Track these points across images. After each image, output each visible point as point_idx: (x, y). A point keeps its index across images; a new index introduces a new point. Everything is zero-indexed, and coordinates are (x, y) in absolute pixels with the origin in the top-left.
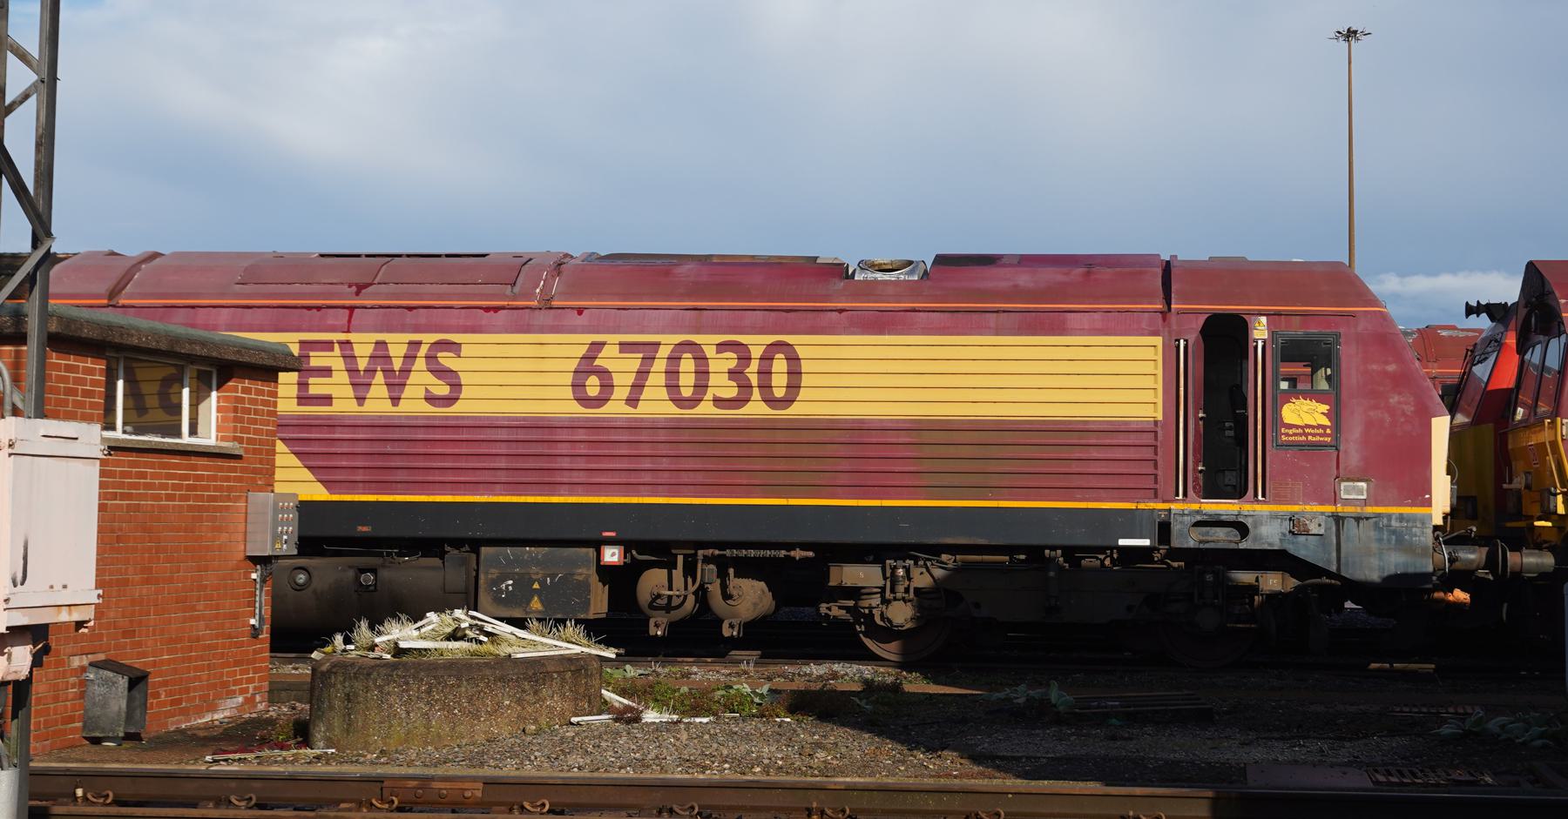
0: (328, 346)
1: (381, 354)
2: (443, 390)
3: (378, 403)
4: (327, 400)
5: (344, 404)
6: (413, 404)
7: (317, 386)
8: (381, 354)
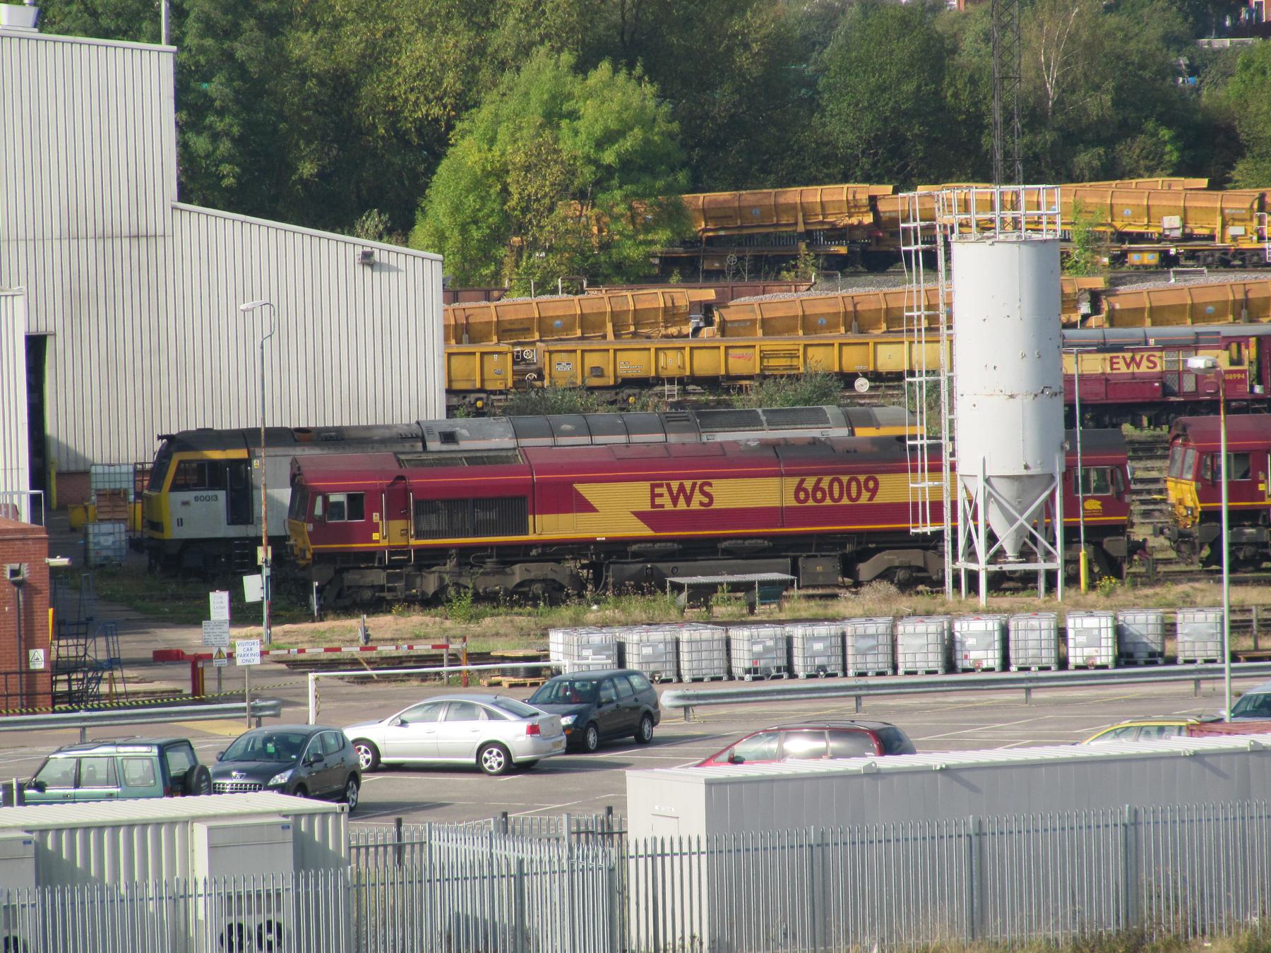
0: (661, 486)
1: (682, 488)
2: (706, 500)
3: (682, 505)
4: (662, 506)
5: (669, 506)
6: (695, 505)
7: (658, 501)
8: (682, 488)
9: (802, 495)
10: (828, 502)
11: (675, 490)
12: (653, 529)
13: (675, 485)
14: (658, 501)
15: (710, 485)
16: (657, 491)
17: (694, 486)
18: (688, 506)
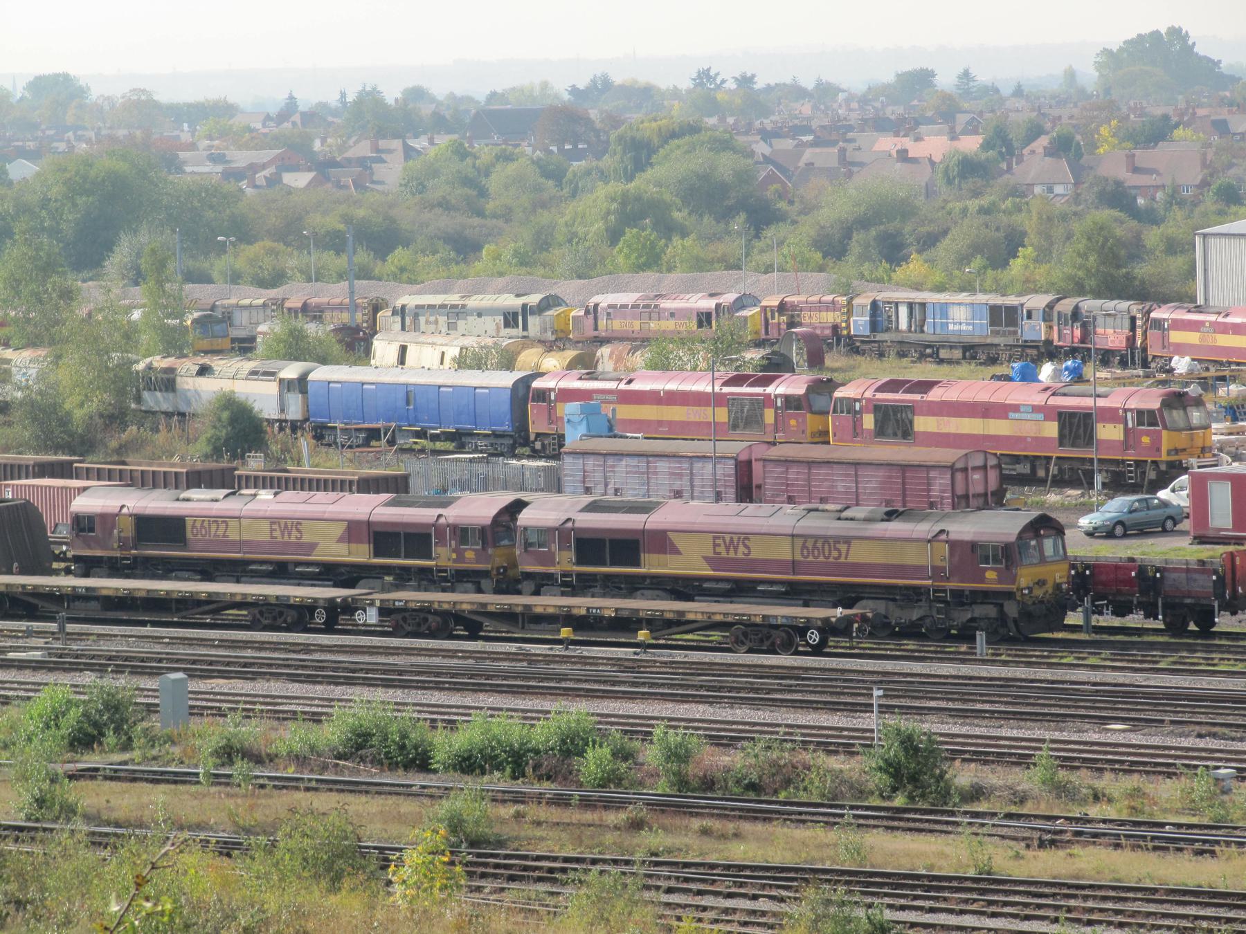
0: (719, 538)
3: (732, 554)
4: (720, 553)
5: (724, 554)
7: (718, 550)
9: (805, 552)
10: (821, 559)
11: (728, 540)
12: (714, 570)
13: (728, 537)
14: (718, 550)
16: (718, 541)
17: (739, 538)
18: (736, 553)
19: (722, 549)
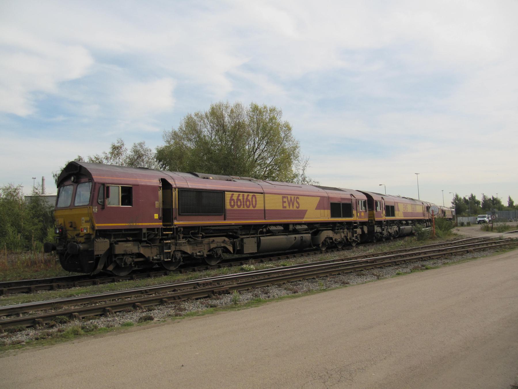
3: (291, 208)
4: (285, 207)
5: (288, 208)
6: (295, 208)
7: (285, 205)
14: (285, 205)
15: (298, 198)
19: (286, 205)
